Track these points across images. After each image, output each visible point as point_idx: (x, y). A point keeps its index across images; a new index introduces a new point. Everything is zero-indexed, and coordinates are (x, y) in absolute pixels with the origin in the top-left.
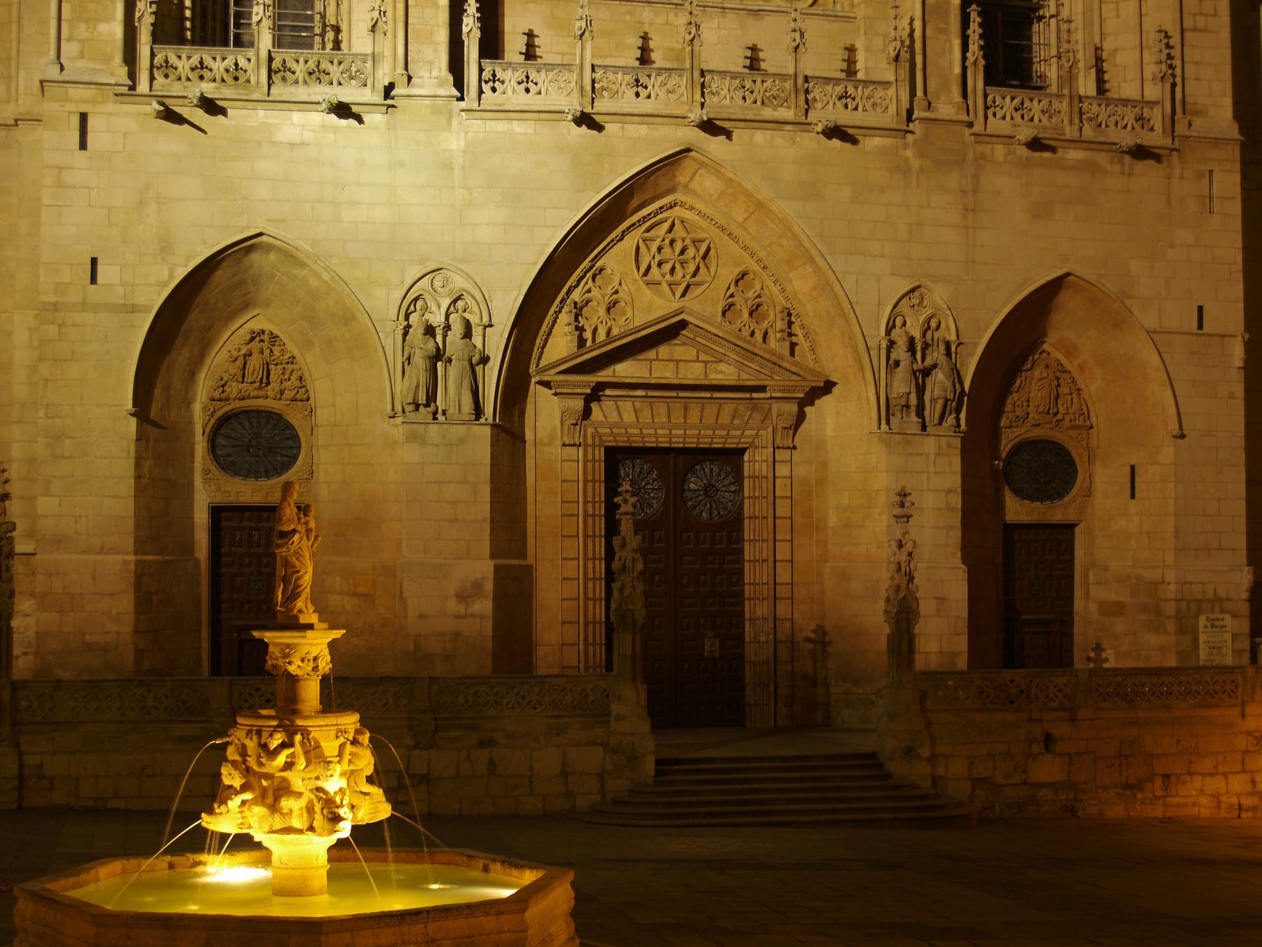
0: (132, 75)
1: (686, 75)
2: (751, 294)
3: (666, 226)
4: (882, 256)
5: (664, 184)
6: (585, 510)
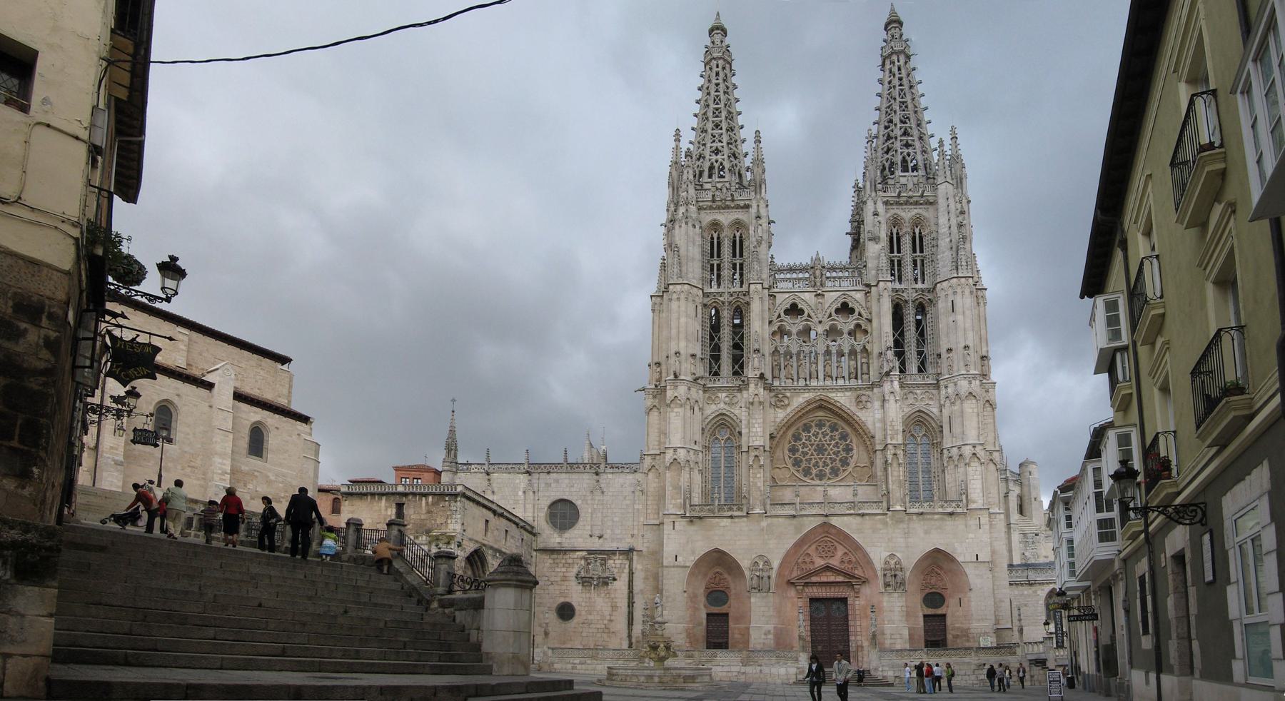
4: (881, 546)
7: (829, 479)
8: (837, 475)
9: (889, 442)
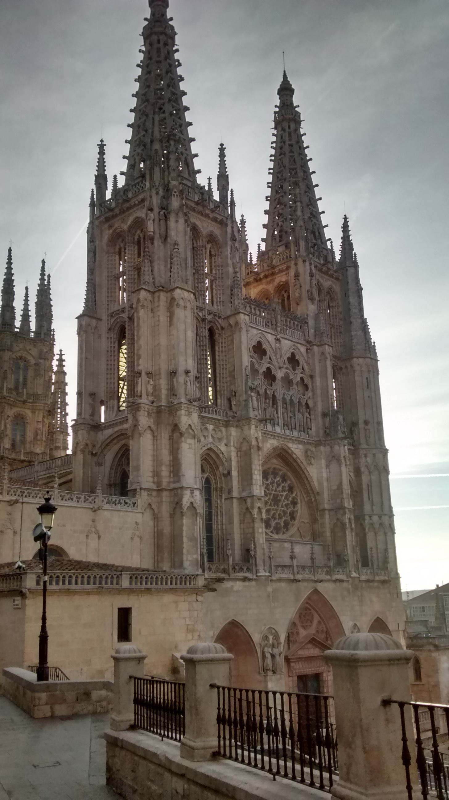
0: (204, 571)
7: (284, 533)
8: (287, 530)
9: (346, 505)
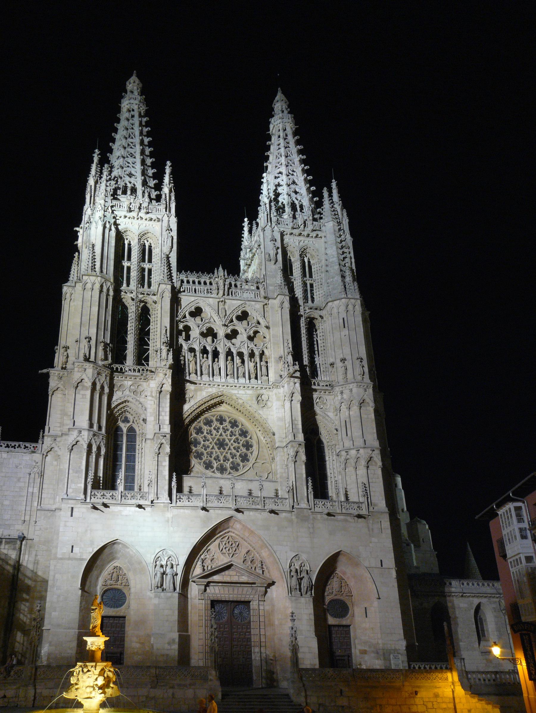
1: (231, 497)
2: (251, 557)
3: (227, 538)
5: (226, 526)
6: (205, 618)
8: (237, 470)
